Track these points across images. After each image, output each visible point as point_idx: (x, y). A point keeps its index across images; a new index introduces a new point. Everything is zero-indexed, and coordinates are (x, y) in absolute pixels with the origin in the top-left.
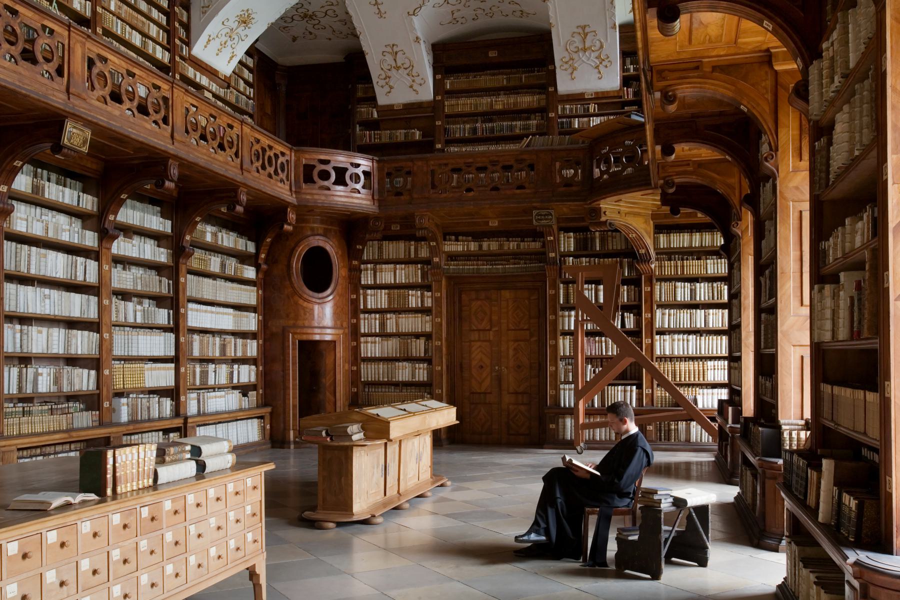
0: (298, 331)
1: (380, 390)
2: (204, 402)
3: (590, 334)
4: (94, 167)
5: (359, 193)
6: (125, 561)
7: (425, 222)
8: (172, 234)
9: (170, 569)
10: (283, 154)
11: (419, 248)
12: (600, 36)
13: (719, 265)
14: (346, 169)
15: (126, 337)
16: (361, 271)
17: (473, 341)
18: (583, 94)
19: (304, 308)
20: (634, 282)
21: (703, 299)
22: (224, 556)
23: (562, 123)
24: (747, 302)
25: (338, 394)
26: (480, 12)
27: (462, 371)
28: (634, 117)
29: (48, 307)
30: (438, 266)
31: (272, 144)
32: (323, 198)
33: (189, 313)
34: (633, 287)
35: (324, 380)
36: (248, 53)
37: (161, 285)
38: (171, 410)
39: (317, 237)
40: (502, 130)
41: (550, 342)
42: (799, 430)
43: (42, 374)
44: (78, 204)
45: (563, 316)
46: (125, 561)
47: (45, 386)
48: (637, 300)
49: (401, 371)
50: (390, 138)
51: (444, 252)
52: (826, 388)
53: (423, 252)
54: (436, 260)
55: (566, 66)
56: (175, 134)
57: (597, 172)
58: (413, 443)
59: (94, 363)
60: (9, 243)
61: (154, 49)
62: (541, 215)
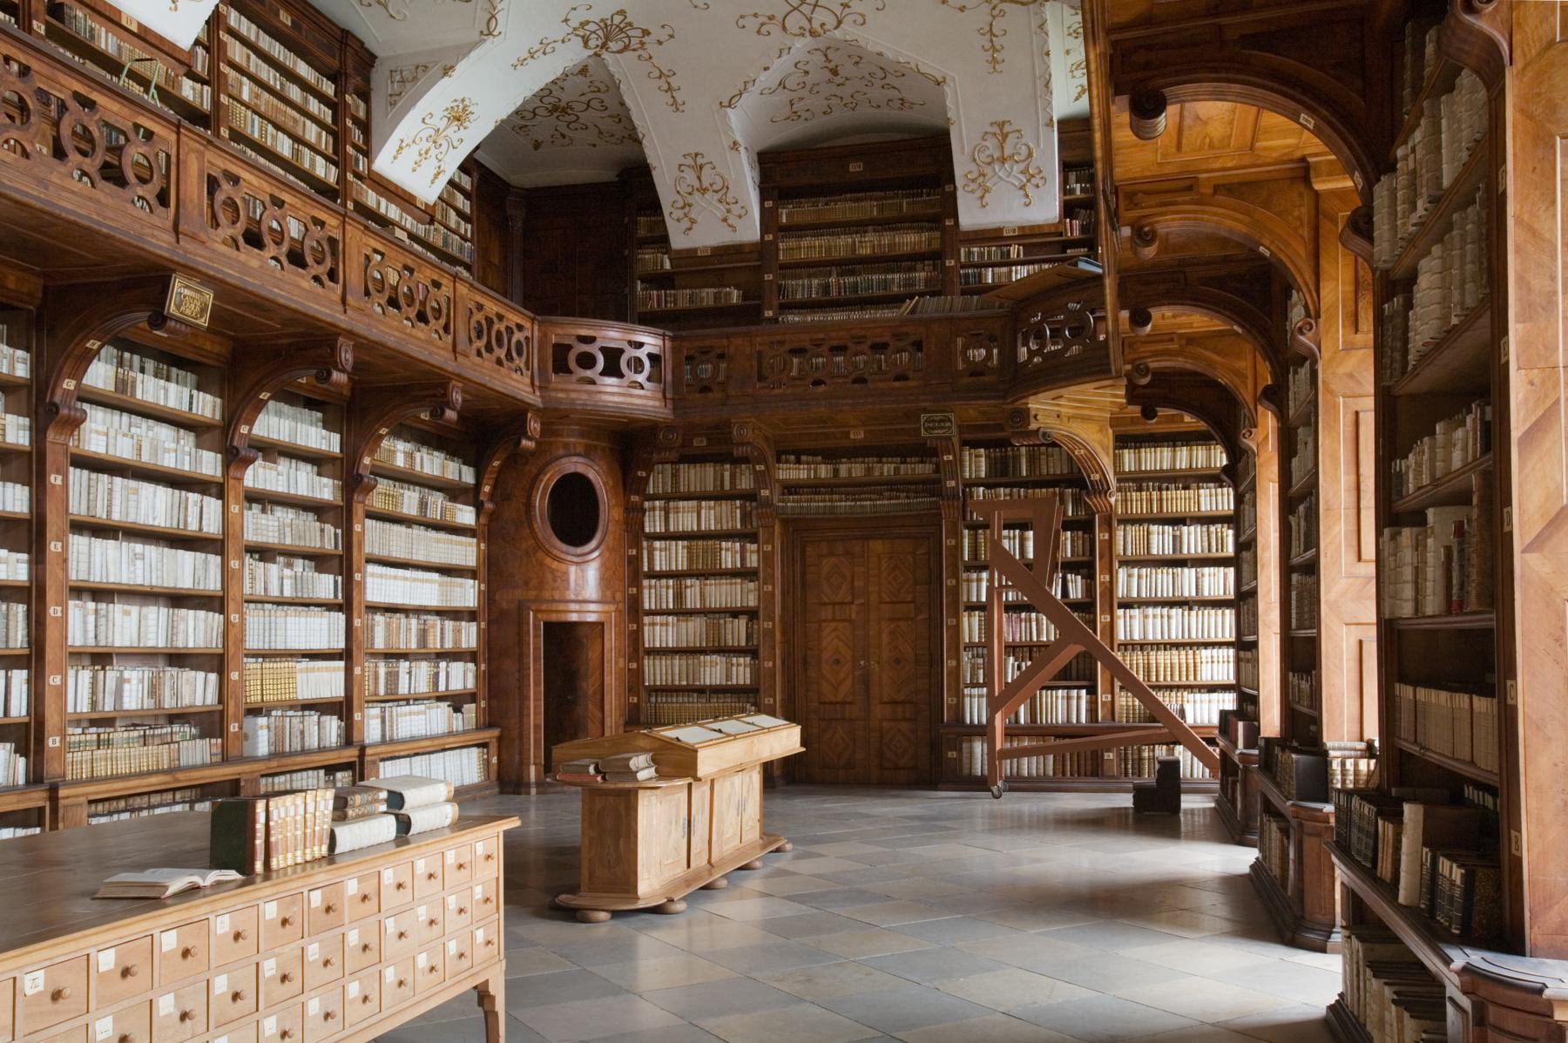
0: (544, 607)
1: (674, 700)
2: (392, 722)
3: (1011, 608)
4: (217, 349)
5: (642, 388)
6: (284, 978)
7: (748, 434)
8: (340, 456)
9: (354, 990)
10: (520, 327)
12: (1028, 138)
13: (1220, 497)
14: (621, 351)
15: (267, 619)
16: (644, 511)
17: (825, 621)
19: (553, 571)
20: (1083, 526)
21: (1193, 551)
22: (440, 966)
24: (1266, 555)
25: (607, 707)
26: (834, 101)
27: (805, 668)
28: (1083, 266)
29: (139, 572)
30: (768, 503)
31: (502, 311)
32: (585, 397)
33: (369, 580)
34: (1080, 533)
35: (584, 685)
36: (464, 168)
37: (324, 537)
38: (339, 736)
39: (575, 459)
41: (948, 621)
42: (1356, 758)
43: (129, 681)
44: (191, 409)
45: (969, 581)
46: (284, 978)
47: (134, 699)
48: (1088, 553)
49: (708, 669)
50: (691, 301)
51: (778, 481)
52: (1405, 692)
54: (765, 493)
55: (973, 186)
56: (349, 298)
57: (1023, 353)
58: (733, 784)
59: (216, 662)
60: (78, 471)
61: (313, 162)
62: (934, 421)
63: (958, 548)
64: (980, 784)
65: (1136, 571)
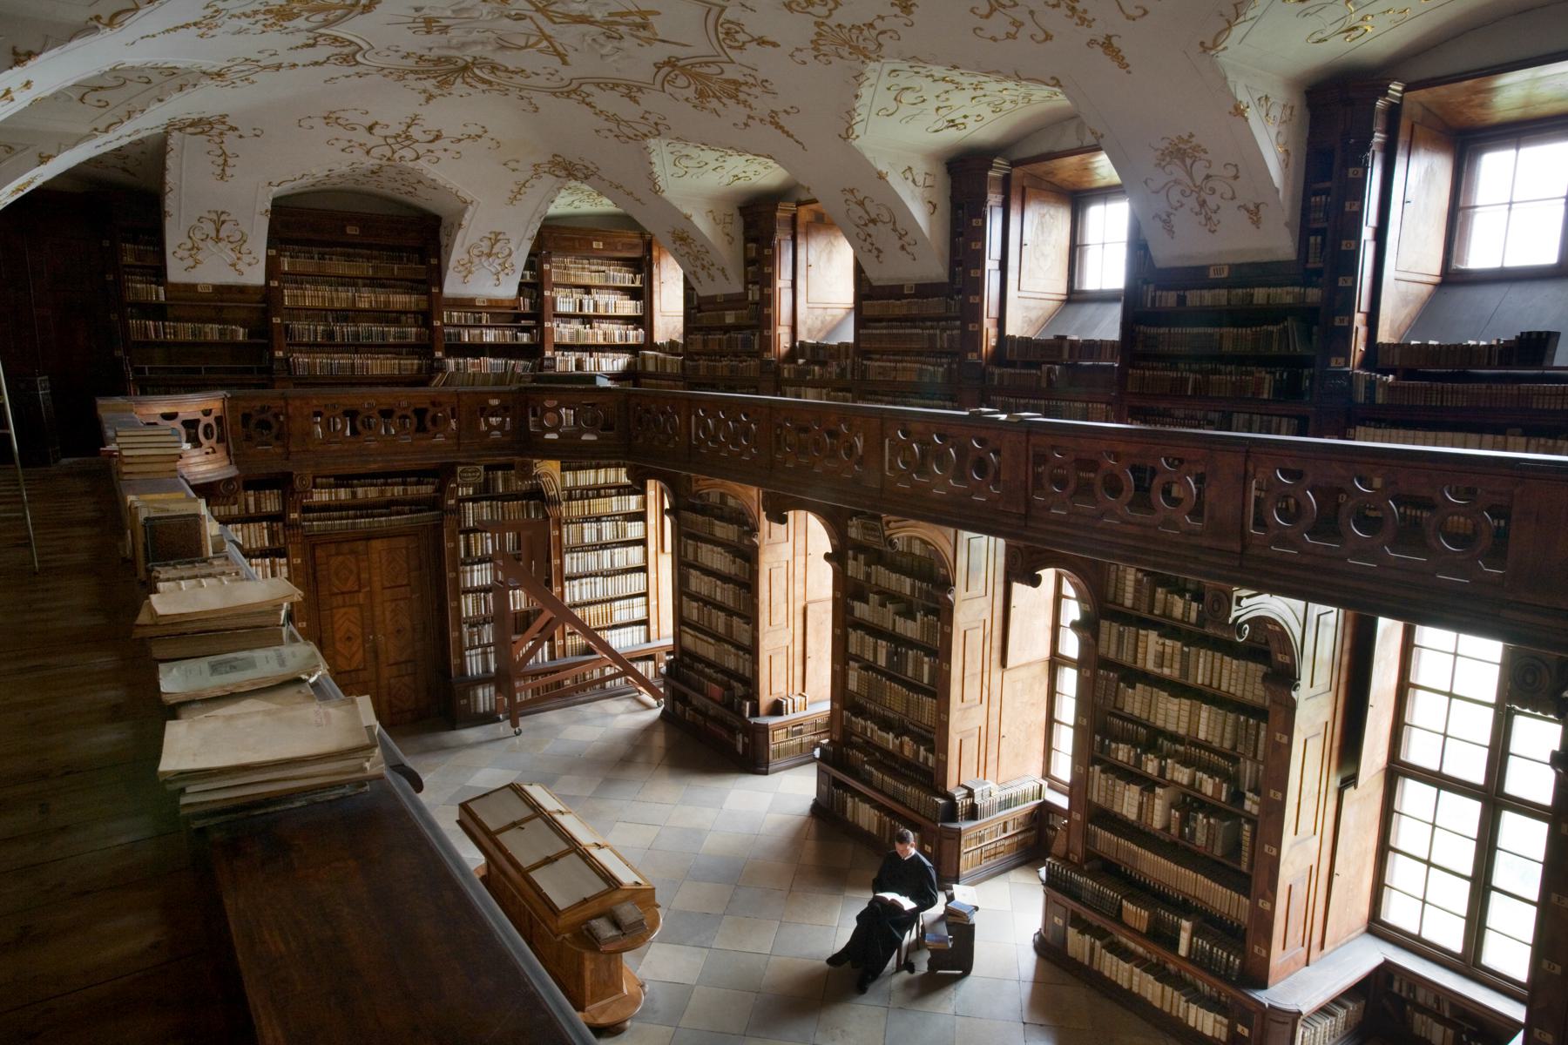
11: (263, 500)
18: (472, 300)
23: (449, 334)
40: (370, 336)
41: (451, 604)
53: (268, 504)
54: (294, 516)
55: (461, 268)
63: (457, 548)
64: (489, 718)
65: (575, 555)
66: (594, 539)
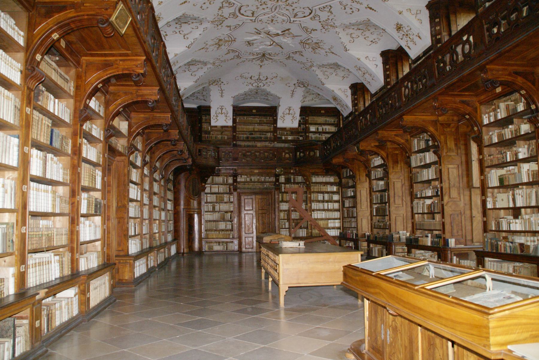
63: (279, 198)
66: (322, 199)
